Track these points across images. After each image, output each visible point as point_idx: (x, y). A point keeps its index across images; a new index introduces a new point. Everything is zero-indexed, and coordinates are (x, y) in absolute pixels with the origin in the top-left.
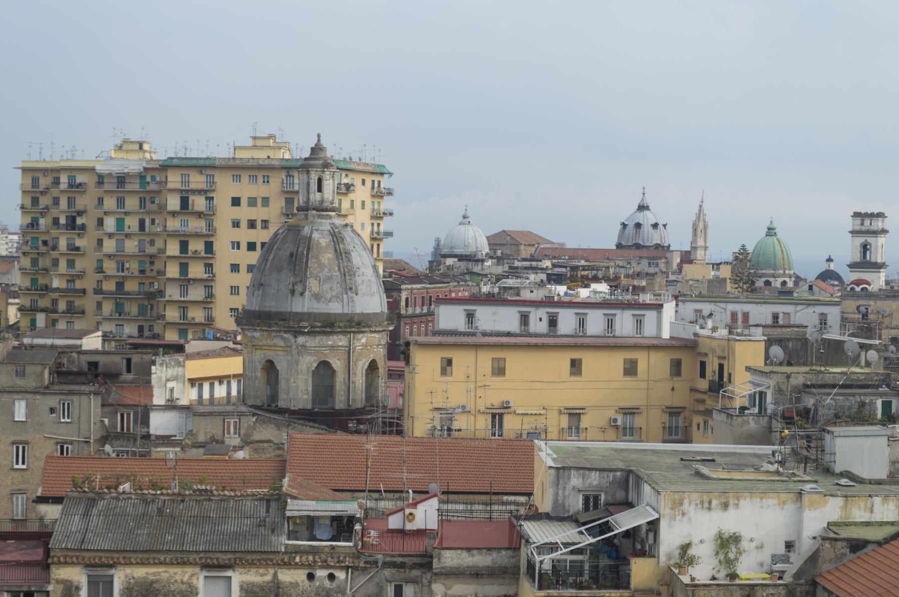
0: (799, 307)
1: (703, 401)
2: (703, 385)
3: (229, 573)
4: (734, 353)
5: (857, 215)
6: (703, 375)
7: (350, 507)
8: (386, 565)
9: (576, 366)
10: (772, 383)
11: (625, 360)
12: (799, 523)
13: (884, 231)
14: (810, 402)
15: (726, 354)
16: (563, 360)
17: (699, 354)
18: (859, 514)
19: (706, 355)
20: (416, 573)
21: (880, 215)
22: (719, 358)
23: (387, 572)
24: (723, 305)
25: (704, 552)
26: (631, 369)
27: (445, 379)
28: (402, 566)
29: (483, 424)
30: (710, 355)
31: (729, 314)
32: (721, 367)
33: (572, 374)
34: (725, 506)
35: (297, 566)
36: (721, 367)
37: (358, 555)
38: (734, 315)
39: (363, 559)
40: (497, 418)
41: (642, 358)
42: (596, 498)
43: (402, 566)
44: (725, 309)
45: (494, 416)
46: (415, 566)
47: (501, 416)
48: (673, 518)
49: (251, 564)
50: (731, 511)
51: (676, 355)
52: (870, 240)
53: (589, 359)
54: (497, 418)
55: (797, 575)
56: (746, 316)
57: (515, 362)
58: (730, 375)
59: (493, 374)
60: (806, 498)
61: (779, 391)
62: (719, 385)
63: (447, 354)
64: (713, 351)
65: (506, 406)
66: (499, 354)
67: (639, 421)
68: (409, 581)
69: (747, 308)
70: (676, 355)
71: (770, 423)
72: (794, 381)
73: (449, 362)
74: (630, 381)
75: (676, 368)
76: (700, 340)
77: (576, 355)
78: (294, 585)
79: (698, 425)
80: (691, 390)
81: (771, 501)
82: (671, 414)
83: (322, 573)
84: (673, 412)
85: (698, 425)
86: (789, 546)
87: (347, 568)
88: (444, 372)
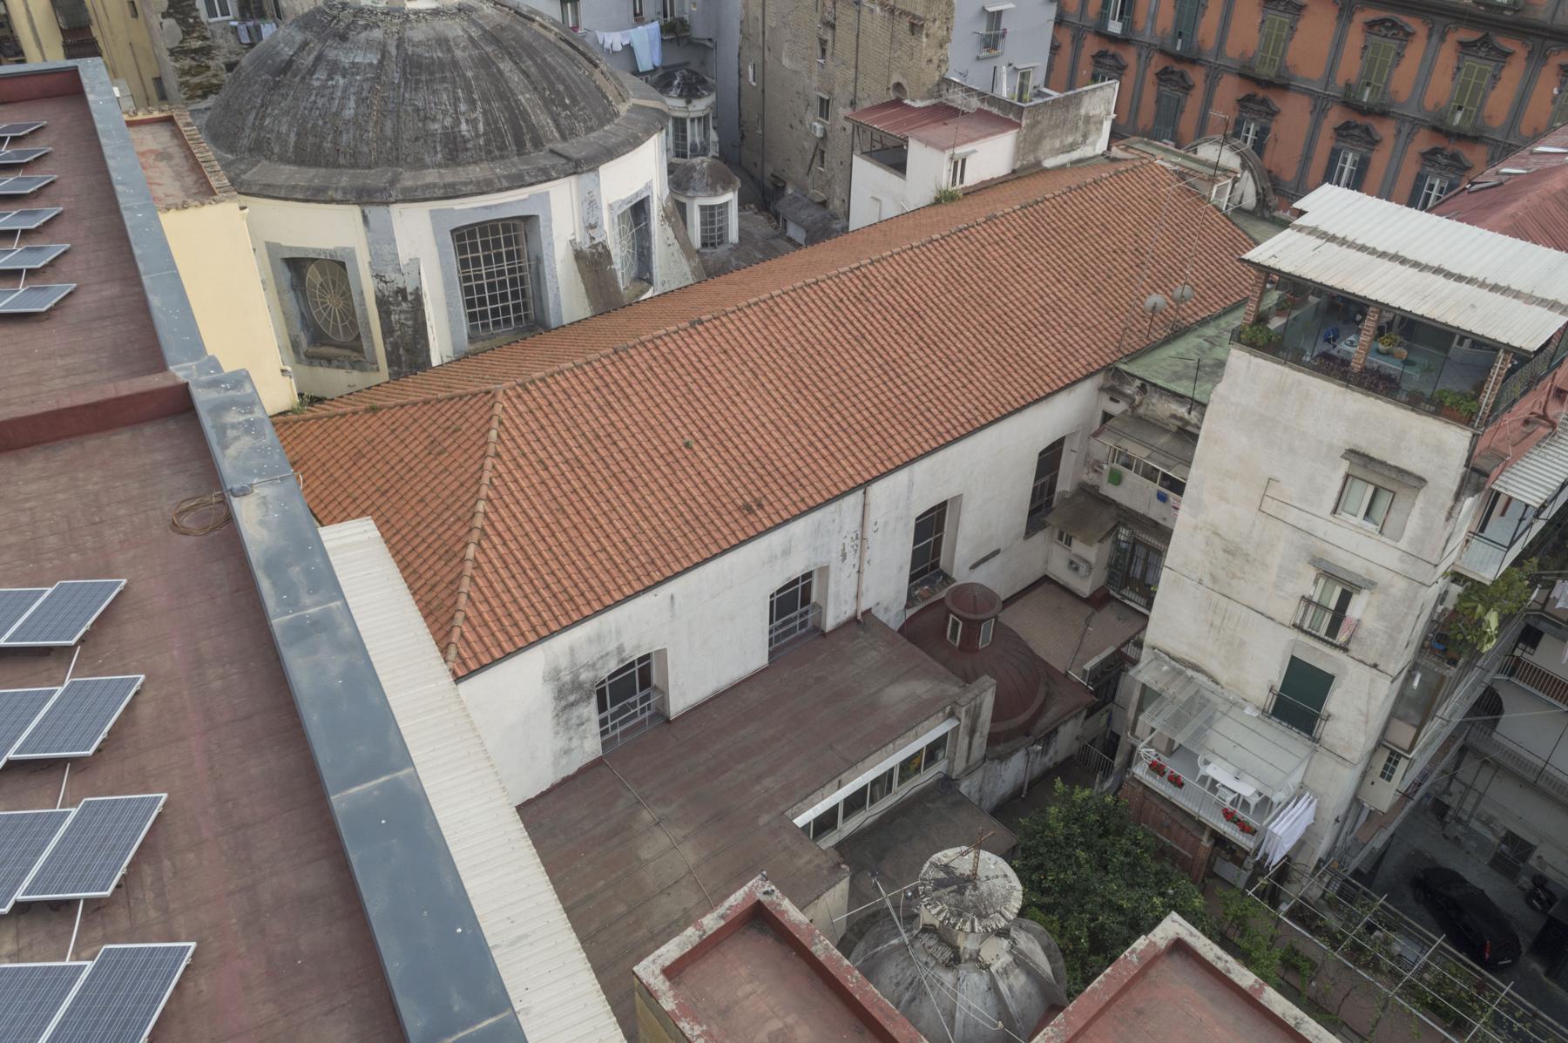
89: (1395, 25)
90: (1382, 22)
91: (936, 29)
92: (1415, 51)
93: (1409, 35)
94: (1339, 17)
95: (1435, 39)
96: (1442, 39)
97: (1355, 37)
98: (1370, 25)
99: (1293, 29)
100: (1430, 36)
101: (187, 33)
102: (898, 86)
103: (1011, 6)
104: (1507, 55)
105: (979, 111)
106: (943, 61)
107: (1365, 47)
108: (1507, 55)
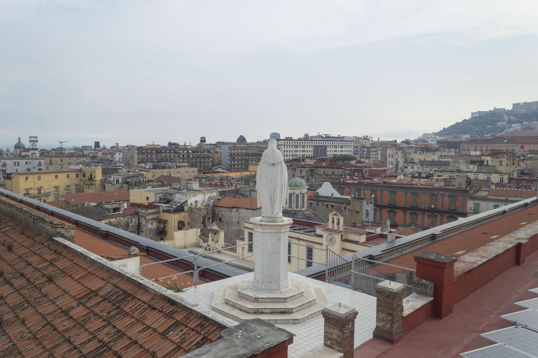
0: (33, 160)
1: (85, 182)
2: (87, 178)
3: (102, 221)
4: (95, 171)
5: (30, 137)
6: (84, 176)
7: (115, 206)
8: (130, 215)
9: (56, 176)
10: (121, 177)
11: (67, 175)
12: (205, 198)
13: (38, 141)
14: (129, 180)
15: (93, 172)
16: (54, 175)
17: (83, 172)
18: (212, 195)
19: (85, 172)
20: (134, 216)
21: (37, 137)
22: (90, 173)
23: (130, 217)
24: (11, 160)
25: (193, 204)
26: (68, 177)
27: (26, 182)
28: (132, 215)
29: (37, 191)
30: (87, 173)
31: (13, 163)
32: (91, 175)
33: (56, 179)
34: (196, 196)
35: (115, 218)
36: (91, 175)
37: (124, 214)
38: (15, 163)
39: (125, 215)
40: (39, 190)
41: (70, 174)
42: (161, 198)
43: (132, 215)
44: (12, 161)
45: (38, 189)
46: (134, 215)
47: (40, 189)
48: (189, 199)
49: (106, 219)
50: (196, 197)
51: (77, 173)
52: (35, 143)
53: (59, 175)
54: (39, 190)
55: (212, 205)
56: (18, 163)
57: (43, 177)
58: (94, 176)
59: (38, 180)
60: (205, 194)
61: (122, 178)
62: (91, 178)
63: (27, 176)
64: (88, 172)
65: (41, 187)
66: (39, 175)
67: (71, 188)
68: (133, 218)
69: (18, 161)
70: (77, 173)
71: (122, 185)
72: (125, 176)
73: (27, 178)
74: (68, 179)
75: (77, 176)
76: (83, 169)
77: (56, 174)
78: (113, 222)
79: (86, 188)
80: (81, 180)
81: (201, 195)
82: (77, 186)
83: (118, 218)
84: (77, 185)
85: (86, 188)
86: (203, 201)
87: (123, 217)
88: (26, 180)
89: (415, 213)
90: (412, 213)
91: (361, 212)
92: (420, 217)
93: (418, 214)
94: (404, 213)
95: (423, 215)
96: (424, 215)
97: (408, 216)
98: (410, 214)
99: (395, 216)
100: (422, 214)
101: (204, 227)
102: (354, 223)
103: (369, 209)
104: (436, 216)
105: (371, 225)
106: (362, 218)
107: (410, 217)
108: (436, 216)
